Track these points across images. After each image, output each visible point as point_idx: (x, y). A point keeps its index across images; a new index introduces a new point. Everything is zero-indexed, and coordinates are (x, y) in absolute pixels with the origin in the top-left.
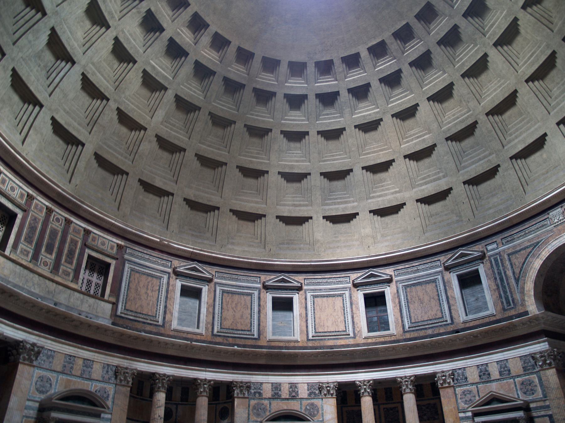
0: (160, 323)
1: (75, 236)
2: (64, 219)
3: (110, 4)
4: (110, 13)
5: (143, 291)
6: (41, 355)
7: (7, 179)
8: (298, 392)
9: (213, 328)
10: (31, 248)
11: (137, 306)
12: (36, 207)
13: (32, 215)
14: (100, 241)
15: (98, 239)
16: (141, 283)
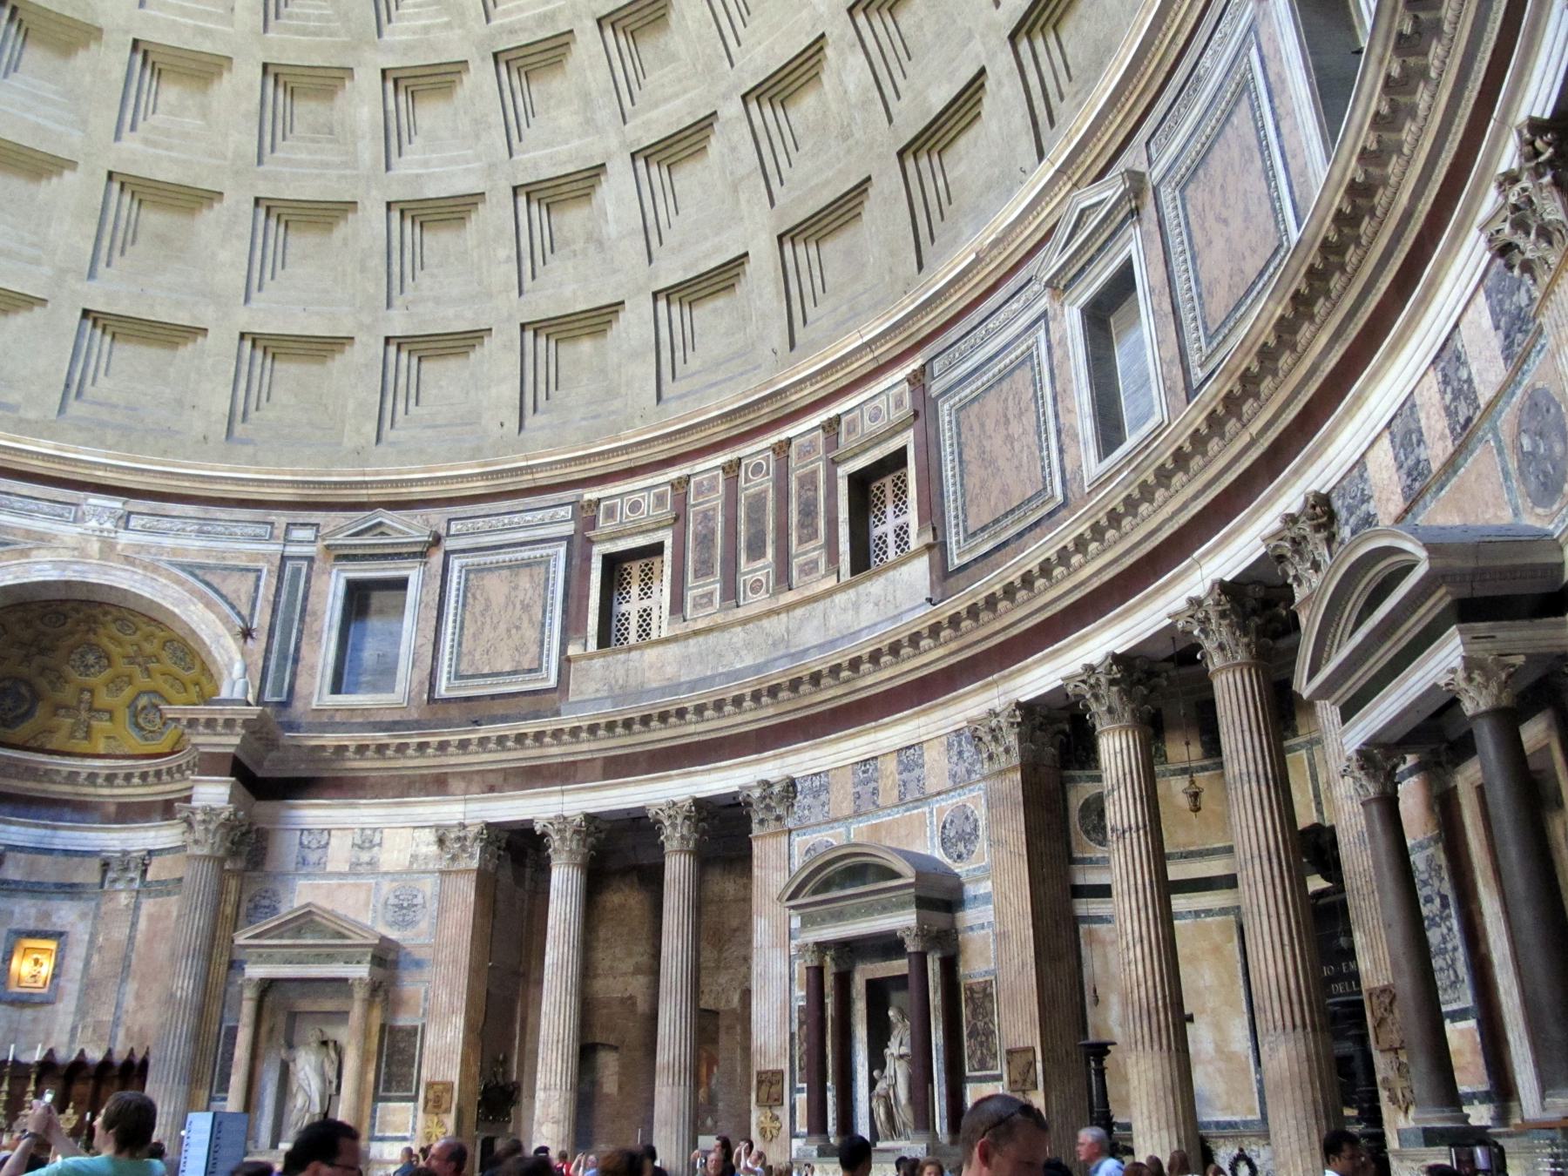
0: (1060, 498)
1: (806, 465)
2: (771, 453)
3: (526, 14)
4: (543, 19)
5: (996, 445)
6: (799, 797)
7: (618, 500)
8: (1469, 381)
9: (1186, 371)
10: (713, 583)
11: (992, 503)
12: (699, 493)
13: (696, 514)
14: (866, 417)
15: (862, 416)
16: (988, 422)
